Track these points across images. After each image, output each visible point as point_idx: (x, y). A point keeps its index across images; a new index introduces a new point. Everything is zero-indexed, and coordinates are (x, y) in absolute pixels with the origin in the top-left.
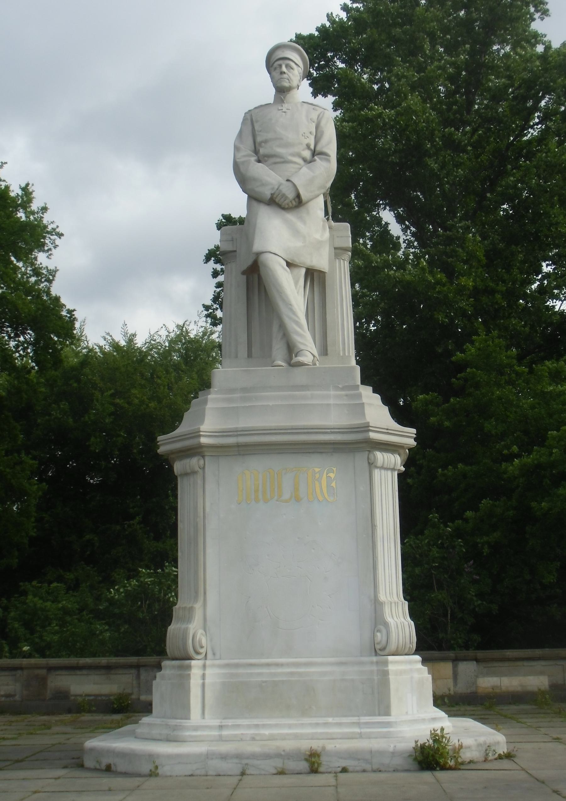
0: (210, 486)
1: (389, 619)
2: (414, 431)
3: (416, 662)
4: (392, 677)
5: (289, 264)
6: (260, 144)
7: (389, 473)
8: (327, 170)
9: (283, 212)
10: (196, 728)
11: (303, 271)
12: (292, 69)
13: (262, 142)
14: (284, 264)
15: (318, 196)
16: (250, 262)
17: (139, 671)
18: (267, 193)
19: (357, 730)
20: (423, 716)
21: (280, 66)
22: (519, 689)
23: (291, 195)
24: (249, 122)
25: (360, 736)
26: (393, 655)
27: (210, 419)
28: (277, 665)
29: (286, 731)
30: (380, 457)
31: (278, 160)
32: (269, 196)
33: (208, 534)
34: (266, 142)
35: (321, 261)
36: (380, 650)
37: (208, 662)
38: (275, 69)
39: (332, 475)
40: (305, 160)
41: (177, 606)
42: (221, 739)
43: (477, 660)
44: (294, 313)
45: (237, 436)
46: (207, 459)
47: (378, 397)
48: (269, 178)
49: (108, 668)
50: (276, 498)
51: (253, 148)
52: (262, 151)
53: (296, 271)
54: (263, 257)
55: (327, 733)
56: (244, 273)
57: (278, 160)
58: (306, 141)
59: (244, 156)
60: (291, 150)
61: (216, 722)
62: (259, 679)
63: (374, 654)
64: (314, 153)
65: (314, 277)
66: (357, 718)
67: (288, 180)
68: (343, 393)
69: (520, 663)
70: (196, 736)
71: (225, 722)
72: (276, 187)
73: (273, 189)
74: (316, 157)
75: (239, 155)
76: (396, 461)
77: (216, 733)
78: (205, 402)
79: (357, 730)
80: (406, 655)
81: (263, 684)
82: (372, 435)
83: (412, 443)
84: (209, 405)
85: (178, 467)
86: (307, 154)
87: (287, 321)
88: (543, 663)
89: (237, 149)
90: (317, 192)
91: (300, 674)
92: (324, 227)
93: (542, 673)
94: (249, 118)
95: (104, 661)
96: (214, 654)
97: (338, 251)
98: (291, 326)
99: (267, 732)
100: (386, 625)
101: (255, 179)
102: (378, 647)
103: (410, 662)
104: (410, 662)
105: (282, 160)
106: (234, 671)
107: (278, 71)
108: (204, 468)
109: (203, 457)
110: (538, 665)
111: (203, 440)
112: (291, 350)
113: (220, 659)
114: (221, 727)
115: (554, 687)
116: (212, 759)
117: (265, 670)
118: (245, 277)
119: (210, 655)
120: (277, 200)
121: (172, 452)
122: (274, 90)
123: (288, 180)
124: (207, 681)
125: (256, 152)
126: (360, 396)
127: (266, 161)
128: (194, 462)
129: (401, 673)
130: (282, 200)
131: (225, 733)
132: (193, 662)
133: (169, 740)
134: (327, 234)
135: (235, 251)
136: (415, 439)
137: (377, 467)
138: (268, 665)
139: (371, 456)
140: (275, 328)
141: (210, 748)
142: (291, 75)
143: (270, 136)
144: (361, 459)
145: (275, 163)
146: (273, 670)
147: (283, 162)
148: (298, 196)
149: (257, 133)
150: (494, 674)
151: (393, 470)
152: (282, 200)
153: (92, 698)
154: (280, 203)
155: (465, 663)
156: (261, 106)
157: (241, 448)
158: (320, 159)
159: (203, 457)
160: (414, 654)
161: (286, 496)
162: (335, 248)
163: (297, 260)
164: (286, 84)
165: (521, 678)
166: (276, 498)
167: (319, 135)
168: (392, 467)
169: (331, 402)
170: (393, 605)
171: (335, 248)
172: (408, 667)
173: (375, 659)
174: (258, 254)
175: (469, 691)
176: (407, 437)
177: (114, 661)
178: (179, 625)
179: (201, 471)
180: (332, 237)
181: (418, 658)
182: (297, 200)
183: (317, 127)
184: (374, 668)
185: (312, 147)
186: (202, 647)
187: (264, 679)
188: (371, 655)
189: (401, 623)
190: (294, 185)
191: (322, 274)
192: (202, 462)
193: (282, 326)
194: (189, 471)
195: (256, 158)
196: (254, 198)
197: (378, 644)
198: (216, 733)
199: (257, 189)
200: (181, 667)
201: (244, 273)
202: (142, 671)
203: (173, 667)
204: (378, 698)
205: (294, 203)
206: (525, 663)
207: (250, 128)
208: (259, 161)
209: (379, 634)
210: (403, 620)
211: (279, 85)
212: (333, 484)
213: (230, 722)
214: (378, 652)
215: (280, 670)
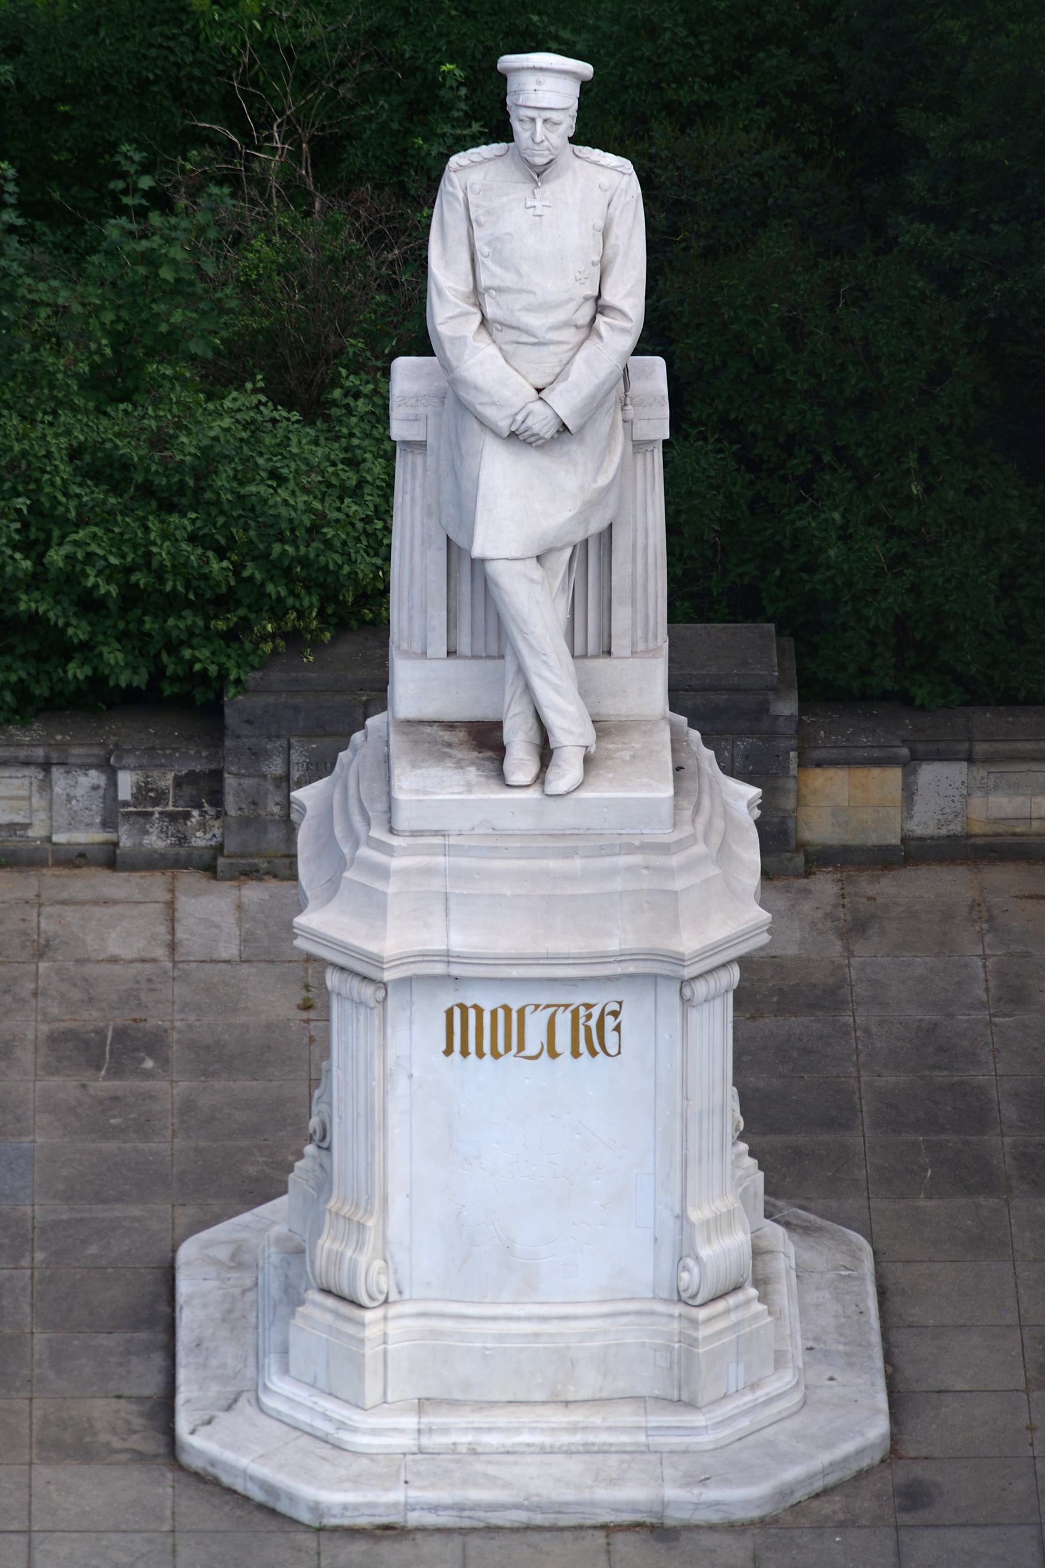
31: (525, 338)
33: (390, 1107)
37: (392, 1311)
57: (525, 338)
63: (676, 1298)
81: (488, 1352)
96: (400, 1292)
100: (697, 1259)
138: (494, 1318)
161: (532, 1047)
166: (514, 1049)
173: (677, 1309)
192: (381, 994)
197: (686, 1290)
209: (685, 1275)
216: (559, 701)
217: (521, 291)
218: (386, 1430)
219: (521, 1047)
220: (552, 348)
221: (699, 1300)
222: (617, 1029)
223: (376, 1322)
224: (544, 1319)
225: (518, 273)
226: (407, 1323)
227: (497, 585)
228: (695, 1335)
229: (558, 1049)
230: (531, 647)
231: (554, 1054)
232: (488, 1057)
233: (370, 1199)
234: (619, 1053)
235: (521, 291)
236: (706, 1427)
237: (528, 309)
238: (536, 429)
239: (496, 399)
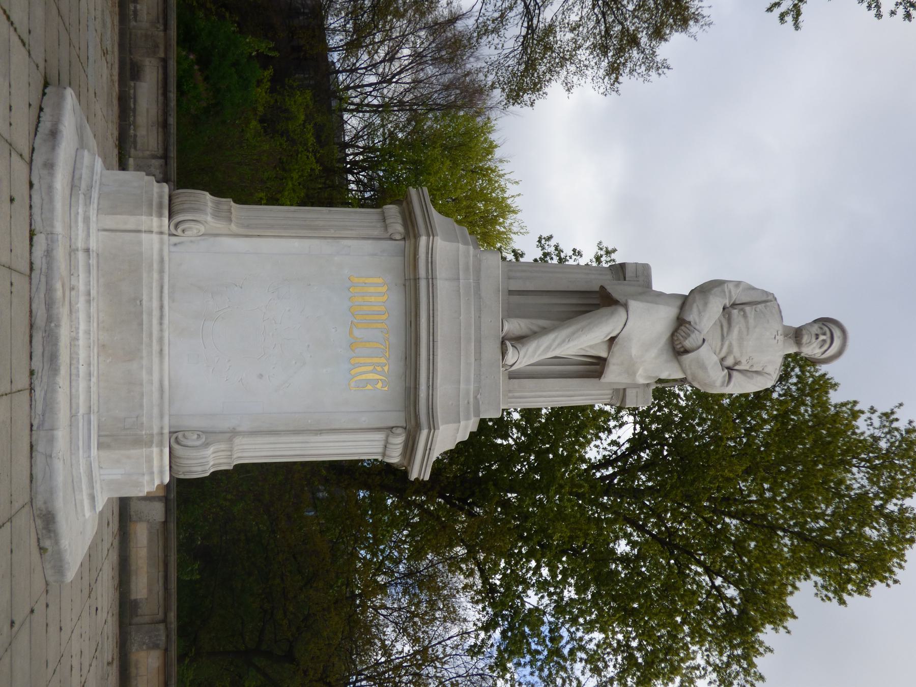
0: (368, 246)
1: (211, 449)
2: (427, 478)
4: (144, 451)
5: (612, 340)
6: (742, 310)
7: (380, 450)
8: (714, 382)
9: (668, 334)
10: (87, 220)
11: (604, 354)
12: (821, 347)
13: (744, 312)
14: (613, 335)
15: (684, 372)
16: (615, 295)
17: (161, 158)
18: (692, 316)
19: (82, 410)
20: (97, 486)
21: (824, 334)
22: (133, 568)
23: (688, 344)
24: (764, 298)
25: (73, 416)
26: (170, 452)
27: (446, 246)
28: (161, 317)
29: (82, 327)
30: (398, 441)
31: (725, 330)
32: (688, 319)
34: (745, 316)
35: (613, 375)
36: (176, 438)
37: (166, 237)
38: (821, 328)
39: (379, 385)
40: (722, 360)
41: (232, 203)
42: (72, 251)
43: (165, 523)
44: (559, 345)
45: (427, 279)
46: (402, 242)
47: (466, 438)
48: (706, 319)
49: (165, 125)
51: (738, 302)
52: (735, 312)
53: (605, 347)
54: (622, 312)
55: (78, 375)
56: (602, 287)
57: (725, 330)
58: (744, 361)
59: (730, 292)
60: (735, 344)
61: (93, 245)
62: (145, 298)
63: (172, 430)
64: (729, 368)
65: (594, 367)
66: (96, 410)
67: (704, 340)
68: (472, 400)
69: (161, 568)
70: (76, 222)
71: (93, 255)
72: (697, 327)
73: (695, 323)
74: (726, 371)
75: (731, 286)
76: (394, 458)
77: (80, 244)
78: (466, 243)
79: (82, 410)
80: (170, 467)
81: (138, 302)
82: (424, 432)
83: (413, 476)
84: (461, 247)
85: (392, 210)
86: (729, 362)
87: (551, 336)
88: (161, 593)
89: (738, 284)
90: (689, 372)
91: (150, 345)
92: (649, 377)
93: (150, 591)
94: (770, 298)
95: (172, 120)
96: (175, 245)
97: (621, 392)
98: (546, 340)
99: (81, 305)
100: (206, 445)
101: (706, 304)
102: (180, 435)
103: (161, 472)
104: (161, 472)
106: (156, 266)
107: (819, 332)
108: (391, 239)
109: (404, 239)
110: (159, 587)
111: (423, 240)
112: (520, 340)
113: (170, 252)
114: (87, 251)
115: (135, 604)
116: (47, 239)
117: (155, 304)
118: (598, 289)
119: (174, 240)
120: (683, 328)
121: (410, 203)
122: (797, 325)
123: (704, 340)
124: (144, 236)
125: (734, 305)
126: (467, 418)
127: (724, 316)
128: (398, 228)
129: (149, 460)
130: (683, 334)
131: (81, 256)
132: (166, 220)
133: (73, 186)
134: (641, 381)
135: (625, 279)
136: (417, 479)
137: (387, 437)
138: (161, 308)
139: (399, 431)
140: (543, 323)
141: (60, 237)
142: (815, 345)
143: (751, 321)
144: (397, 418)
145: (722, 327)
146: (156, 313)
147: (722, 335)
148: (686, 351)
150: (150, 540)
151: (384, 455)
152: (683, 334)
153: (132, 106)
154: (679, 331)
155: (163, 509)
156: (780, 312)
157: (413, 285)
158: (725, 376)
159: (404, 239)
160: (171, 476)
162: (624, 390)
163: (615, 349)
164: (805, 339)
165: (145, 569)
167: (749, 374)
168: (387, 453)
169: (462, 386)
170: (229, 453)
171: (624, 390)
172: (156, 469)
173: (166, 431)
174: (625, 306)
175: (132, 513)
176: (420, 471)
178: (210, 204)
179: (387, 235)
180: (637, 386)
181: (167, 480)
182: (682, 350)
183: (757, 372)
184: (156, 430)
185: (737, 367)
186: (183, 231)
187: (144, 302)
188: (170, 427)
189: (207, 461)
190: (699, 347)
191: (598, 374)
192: (398, 237)
193: (544, 331)
194: (388, 222)
195: (728, 305)
196: (684, 302)
197: (184, 436)
198: (80, 244)
199: (695, 306)
201: (602, 287)
202: (162, 161)
203: (161, 197)
204: (119, 436)
205: (679, 346)
206: (161, 574)
207: (759, 299)
208: (724, 309)
209: (196, 436)
210: (212, 463)
211: (804, 332)
212: (369, 387)
213: (93, 261)
214: (175, 436)
215: (155, 321)
216: (542, 348)
217: (748, 328)
218: (88, 229)
220: (719, 344)
221: (175, 446)
223: (161, 226)
224: (161, 340)
225: (755, 327)
226: (156, 247)
227: (612, 313)
228: (154, 445)
230: (573, 333)
233: (248, 227)
235: (748, 328)
236: (89, 457)
237: (740, 331)
238: (693, 336)
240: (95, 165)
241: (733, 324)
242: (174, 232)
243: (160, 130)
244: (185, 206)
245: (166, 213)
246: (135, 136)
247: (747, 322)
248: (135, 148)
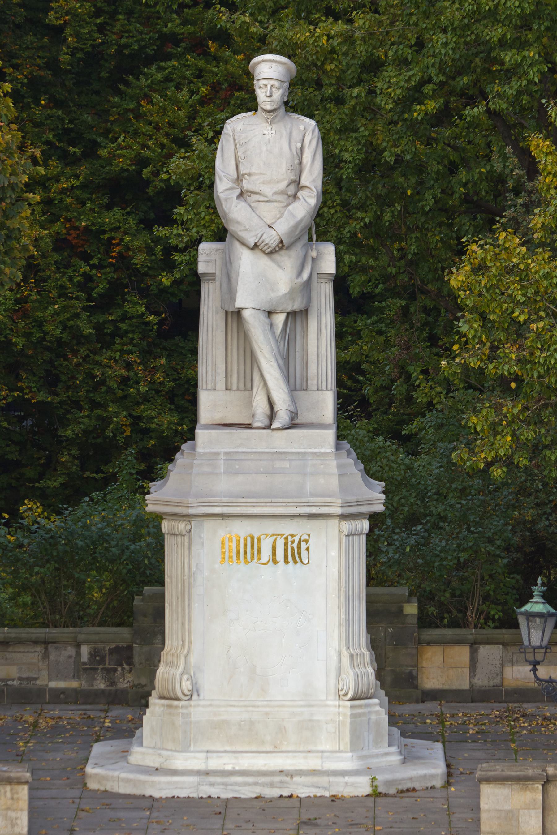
3: (375, 705)
6: (243, 175)
36: (343, 695)
50: (256, 560)
57: (262, 198)
85: (165, 526)
101: (238, 223)
102: (342, 693)
105: (266, 199)
108: (190, 531)
136: (384, 504)
147: (267, 201)
148: (281, 242)
149: (240, 160)
152: (266, 248)
161: (265, 559)
173: (337, 703)
177: (13, 635)
188: (335, 700)
197: (342, 690)
200: (170, 706)
214: (341, 697)
219: (259, 559)
222: (308, 549)
229: (278, 559)
231: (275, 562)
232: (242, 563)
234: (309, 563)
239: (247, 227)
240: (140, 755)
241: (256, 189)
242: (189, 697)
243: (11, 649)
244: (170, 689)
245: (176, 703)
246: (20, 679)
247: (255, 174)
248: (36, 679)
